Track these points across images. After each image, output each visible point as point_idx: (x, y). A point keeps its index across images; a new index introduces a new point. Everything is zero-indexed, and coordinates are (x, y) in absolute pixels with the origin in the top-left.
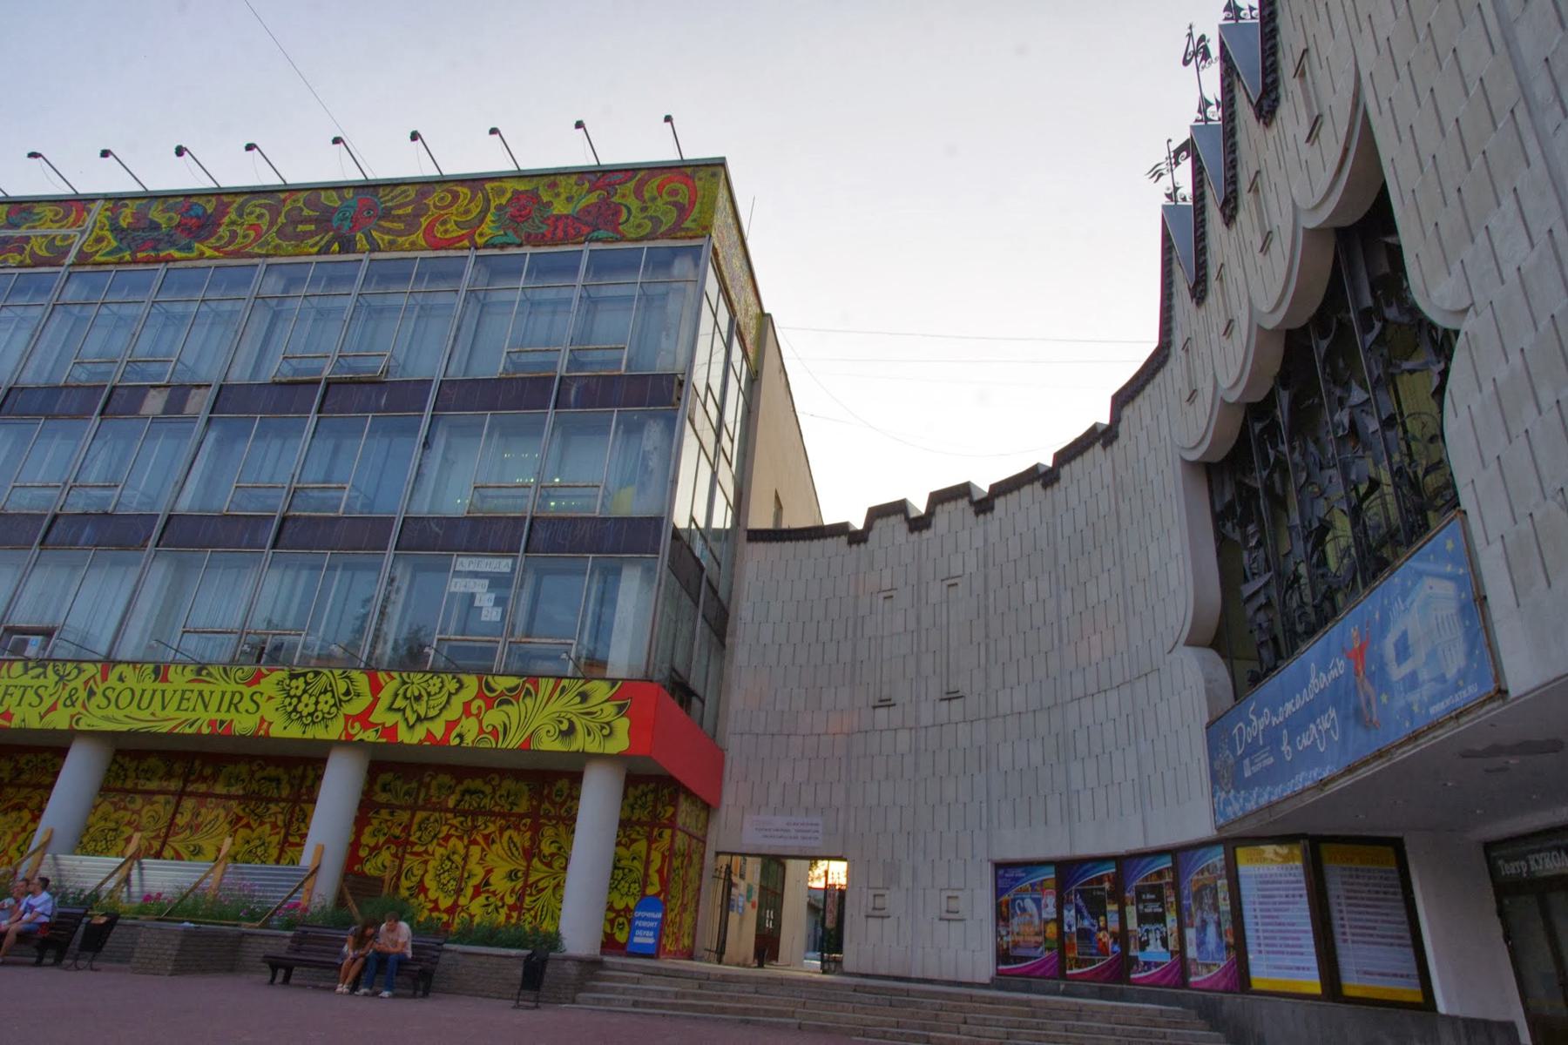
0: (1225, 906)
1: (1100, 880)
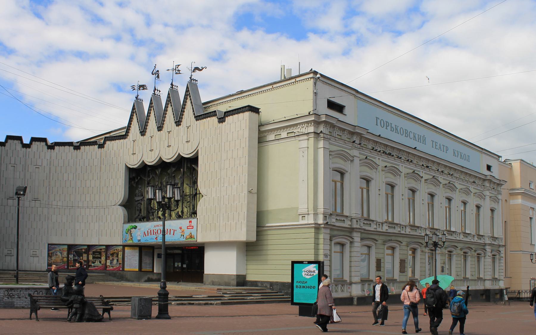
1: (82, 249)
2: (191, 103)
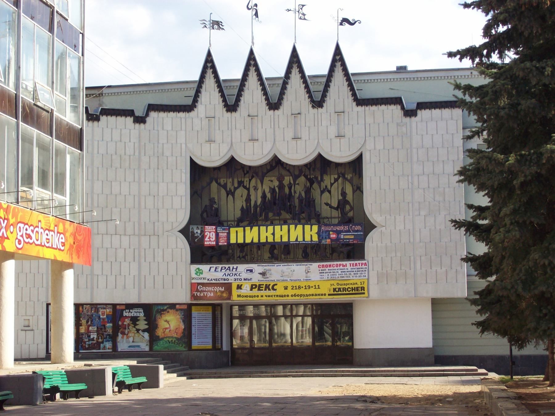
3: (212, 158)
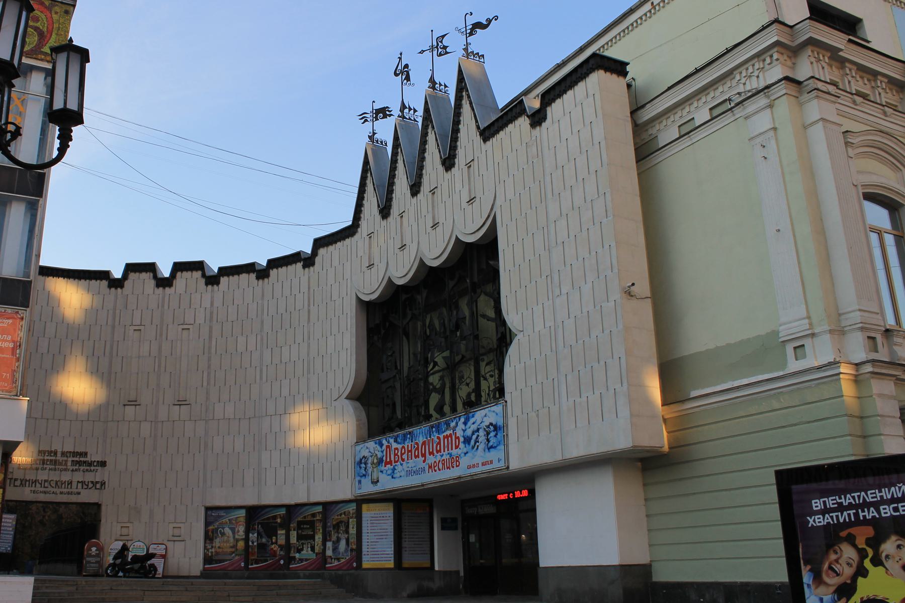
0: (353, 531)
1: (275, 517)
2: (471, 103)
3: (372, 289)
